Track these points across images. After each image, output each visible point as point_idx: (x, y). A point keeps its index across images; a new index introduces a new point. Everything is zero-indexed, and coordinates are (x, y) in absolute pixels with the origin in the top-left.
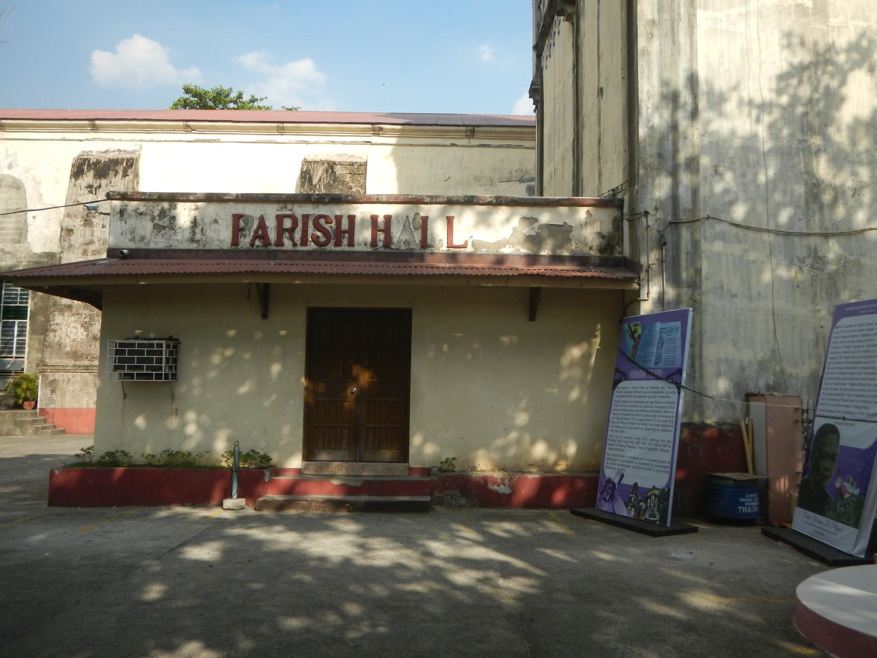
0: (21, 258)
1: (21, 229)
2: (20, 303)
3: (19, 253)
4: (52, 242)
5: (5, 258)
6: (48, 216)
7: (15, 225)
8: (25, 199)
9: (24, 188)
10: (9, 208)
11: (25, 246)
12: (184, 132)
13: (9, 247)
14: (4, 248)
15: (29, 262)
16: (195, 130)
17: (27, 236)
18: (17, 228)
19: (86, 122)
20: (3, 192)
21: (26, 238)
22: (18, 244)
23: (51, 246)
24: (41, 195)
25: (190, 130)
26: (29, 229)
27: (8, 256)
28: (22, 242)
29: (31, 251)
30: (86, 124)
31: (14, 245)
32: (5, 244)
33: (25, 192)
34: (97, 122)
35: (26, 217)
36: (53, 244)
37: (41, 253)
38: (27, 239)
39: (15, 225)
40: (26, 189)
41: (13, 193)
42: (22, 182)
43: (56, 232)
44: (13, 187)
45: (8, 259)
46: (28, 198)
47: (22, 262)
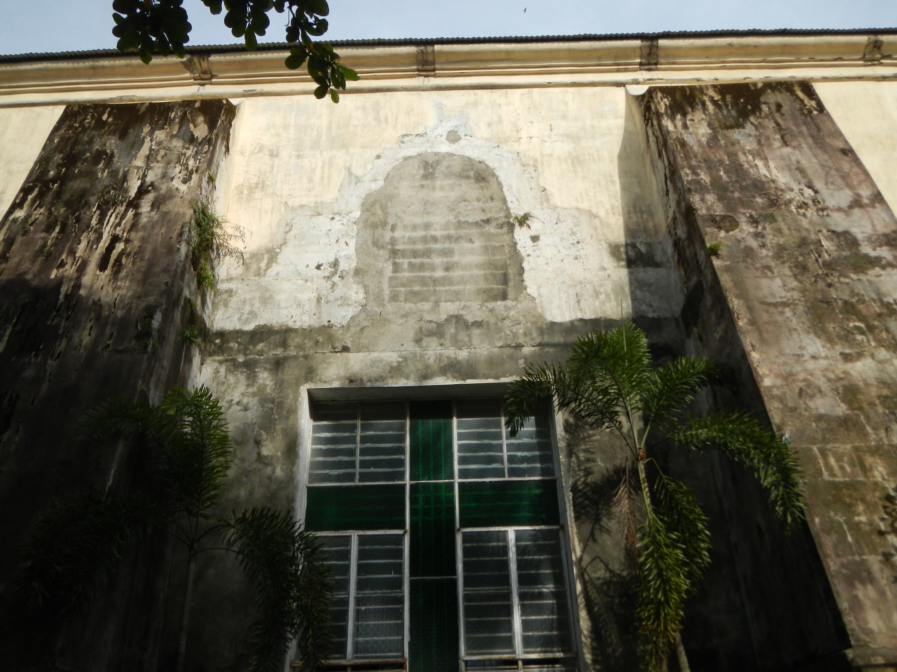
0: (515, 335)
1: (505, 267)
2: (512, 472)
3: (507, 323)
4: (597, 294)
5: (466, 339)
6: (573, 233)
7: (486, 258)
8: (504, 201)
9: (497, 178)
10: (463, 220)
11: (519, 306)
12: (861, 62)
13: (475, 311)
14: (461, 312)
15: (540, 345)
16: (889, 57)
17: (523, 281)
18: (492, 265)
19: (638, 43)
20: (442, 188)
21: (521, 286)
22: (499, 303)
23: (597, 303)
24: (545, 190)
25: (878, 56)
26: (525, 265)
27: (476, 332)
28: (511, 293)
29: (541, 316)
30: (633, 49)
31: (491, 305)
32: (463, 303)
33: (499, 184)
34: (662, 42)
35: (513, 237)
36: (602, 297)
37: (572, 322)
38: (525, 288)
39: (486, 258)
40: (502, 178)
41: (469, 189)
42: (487, 166)
43: (603, 269)
44: (468, 177)
45: (475, 341)
46: (509, 199)
47: (519, 346)
